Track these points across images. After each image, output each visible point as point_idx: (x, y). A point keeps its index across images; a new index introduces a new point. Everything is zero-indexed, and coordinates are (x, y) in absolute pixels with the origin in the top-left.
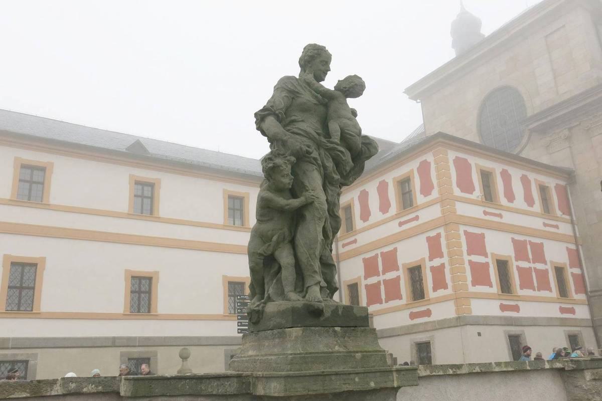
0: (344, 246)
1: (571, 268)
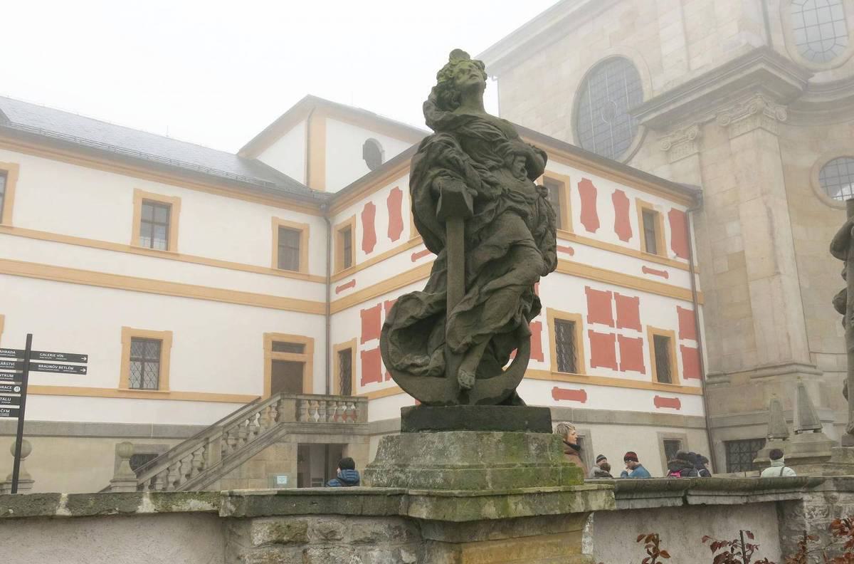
0: (339, 290)
1: (681, 337)
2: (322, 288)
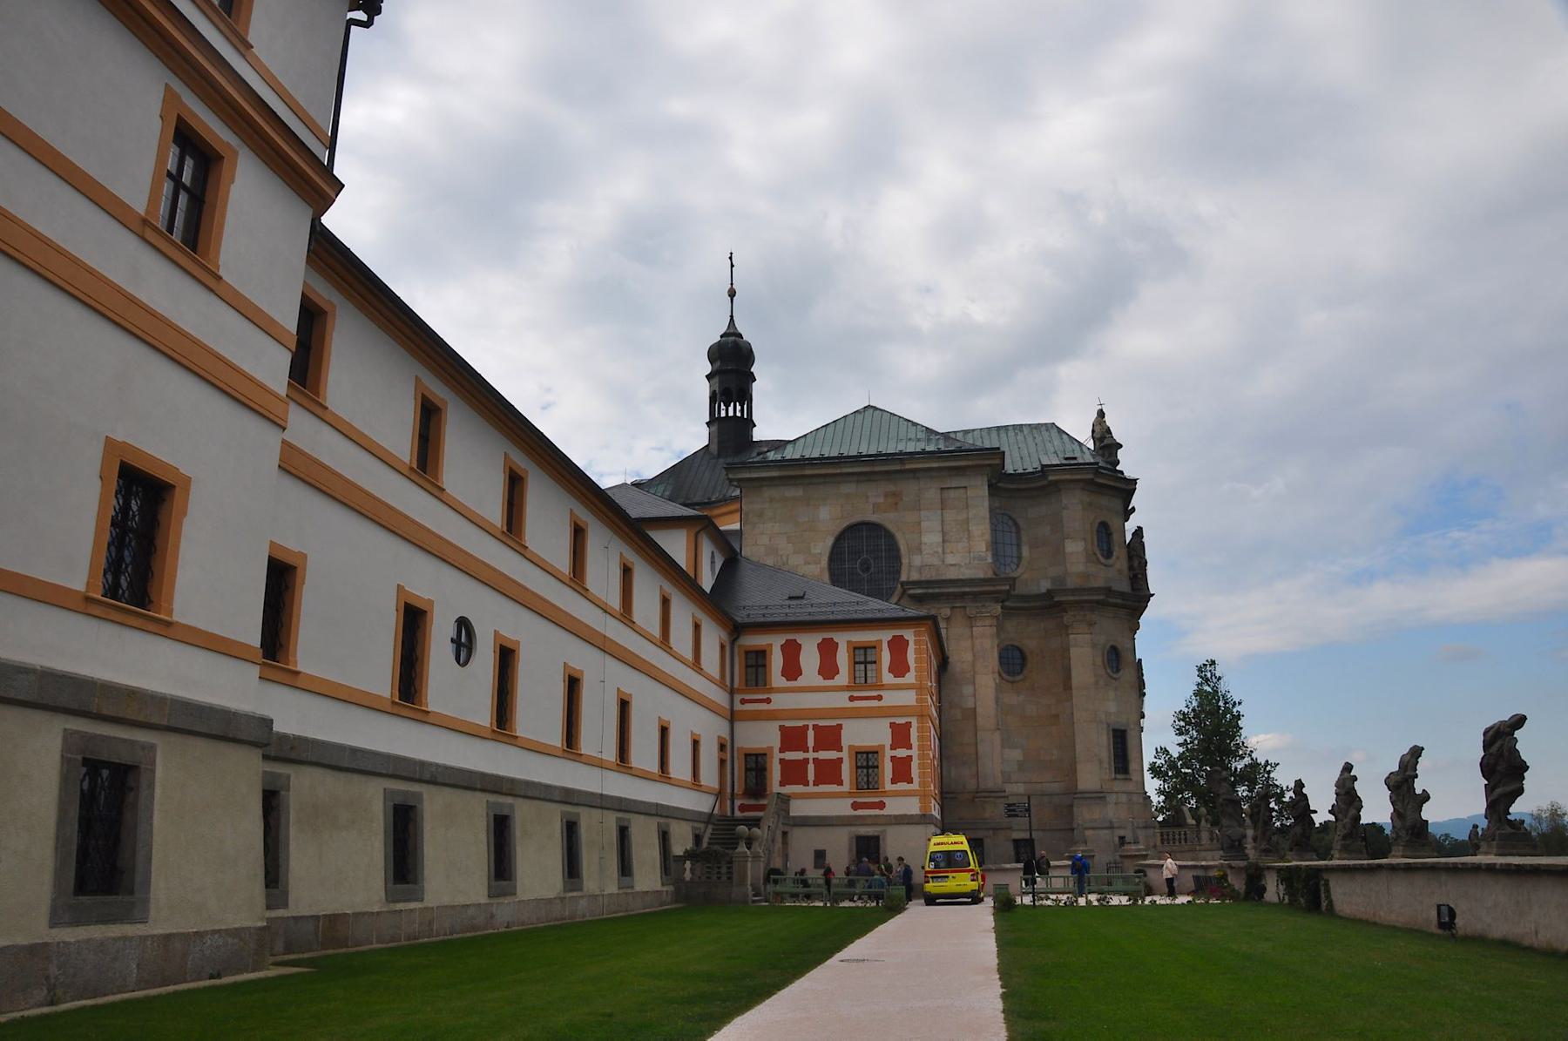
0: (743, 702)
2: (727, 696)
